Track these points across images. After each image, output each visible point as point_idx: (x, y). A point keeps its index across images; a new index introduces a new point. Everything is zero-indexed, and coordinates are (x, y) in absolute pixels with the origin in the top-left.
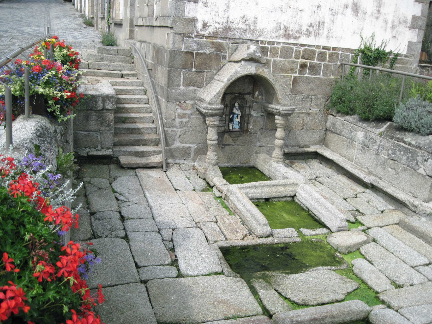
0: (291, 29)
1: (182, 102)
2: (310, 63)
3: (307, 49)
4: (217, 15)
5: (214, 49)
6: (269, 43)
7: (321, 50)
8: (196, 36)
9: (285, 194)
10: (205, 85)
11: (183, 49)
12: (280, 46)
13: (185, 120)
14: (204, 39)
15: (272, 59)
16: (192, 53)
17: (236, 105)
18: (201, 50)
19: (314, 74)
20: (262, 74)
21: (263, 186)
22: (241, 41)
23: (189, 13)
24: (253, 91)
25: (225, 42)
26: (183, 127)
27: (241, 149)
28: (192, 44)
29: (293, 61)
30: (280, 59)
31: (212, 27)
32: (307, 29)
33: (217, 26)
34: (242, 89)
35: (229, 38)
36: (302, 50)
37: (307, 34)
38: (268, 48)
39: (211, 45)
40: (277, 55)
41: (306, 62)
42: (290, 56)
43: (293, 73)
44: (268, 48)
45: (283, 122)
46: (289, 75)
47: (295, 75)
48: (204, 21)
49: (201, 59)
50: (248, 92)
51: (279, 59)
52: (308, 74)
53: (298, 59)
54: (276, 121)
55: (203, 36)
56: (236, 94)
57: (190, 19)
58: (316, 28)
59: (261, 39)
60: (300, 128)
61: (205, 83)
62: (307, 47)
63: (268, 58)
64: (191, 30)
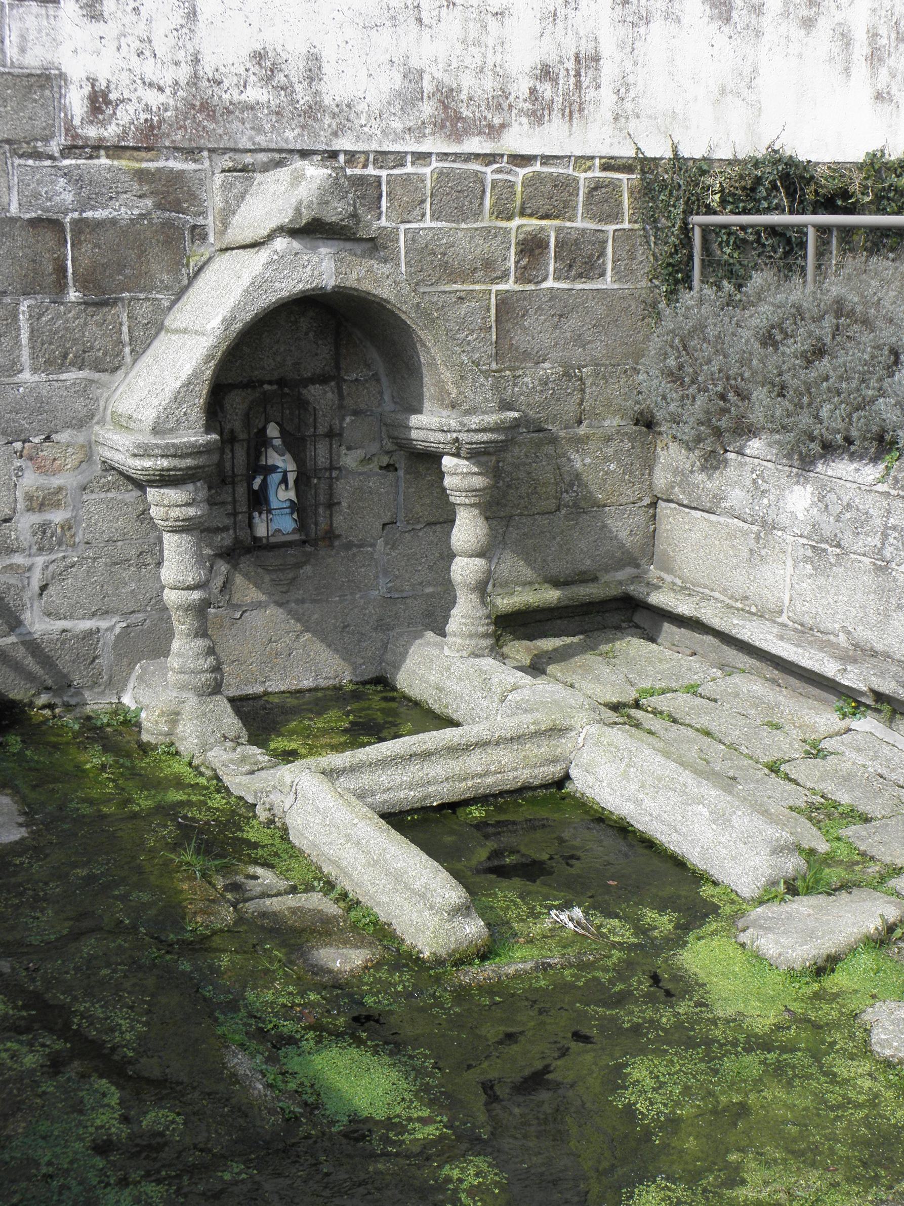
0: (464, 96)
1: (36, 440)
2: (558, 230)
3: (539, 173)
4: (147, 53)
5: (149, 202)
6: (381, 157)
7: (598, 174)
8: (68, 151)
9: (524, 775)
10: (128, 359)
11: (14, 210)
12: (427, 171)
13: (57, 517)
14: (104, 161)
15: (403, 227)
16: (55, 225)
17: (273, 431)
18: (93, 208)
19: (580, 276)
20: (367, 286)
21: (426, 756)
22: (263, 157)
23: (23, 50)
24: (338, 367)
25: (190, 166)
26: (51, 550)
27: (316, 616)
29: (488, 229)
32: (533, 91)
33: (154, 99)
35: (212, 151)
36: (519, 180)
37: (534, 113)
39: (136, 186)
40: (417, 212)
41: (542, 229)
42: (475, 206)
43: (493, 281)
45: (479, 482)
46: (477, 287)
47: (502, 287)
48: (93, 81)
49: (97, 246)
50: (318, 371)
52: (557, 278)
53: (509, 218)
54: (448, 481)
55: (96, 148)
56: (267, 387)
57: (30, 75)
58: (566, 83)
59: (345, 143)
60: (551, 504)
61: (127, 350)
62: (538, 167)
63: (383, 222)
64: (39, 123)
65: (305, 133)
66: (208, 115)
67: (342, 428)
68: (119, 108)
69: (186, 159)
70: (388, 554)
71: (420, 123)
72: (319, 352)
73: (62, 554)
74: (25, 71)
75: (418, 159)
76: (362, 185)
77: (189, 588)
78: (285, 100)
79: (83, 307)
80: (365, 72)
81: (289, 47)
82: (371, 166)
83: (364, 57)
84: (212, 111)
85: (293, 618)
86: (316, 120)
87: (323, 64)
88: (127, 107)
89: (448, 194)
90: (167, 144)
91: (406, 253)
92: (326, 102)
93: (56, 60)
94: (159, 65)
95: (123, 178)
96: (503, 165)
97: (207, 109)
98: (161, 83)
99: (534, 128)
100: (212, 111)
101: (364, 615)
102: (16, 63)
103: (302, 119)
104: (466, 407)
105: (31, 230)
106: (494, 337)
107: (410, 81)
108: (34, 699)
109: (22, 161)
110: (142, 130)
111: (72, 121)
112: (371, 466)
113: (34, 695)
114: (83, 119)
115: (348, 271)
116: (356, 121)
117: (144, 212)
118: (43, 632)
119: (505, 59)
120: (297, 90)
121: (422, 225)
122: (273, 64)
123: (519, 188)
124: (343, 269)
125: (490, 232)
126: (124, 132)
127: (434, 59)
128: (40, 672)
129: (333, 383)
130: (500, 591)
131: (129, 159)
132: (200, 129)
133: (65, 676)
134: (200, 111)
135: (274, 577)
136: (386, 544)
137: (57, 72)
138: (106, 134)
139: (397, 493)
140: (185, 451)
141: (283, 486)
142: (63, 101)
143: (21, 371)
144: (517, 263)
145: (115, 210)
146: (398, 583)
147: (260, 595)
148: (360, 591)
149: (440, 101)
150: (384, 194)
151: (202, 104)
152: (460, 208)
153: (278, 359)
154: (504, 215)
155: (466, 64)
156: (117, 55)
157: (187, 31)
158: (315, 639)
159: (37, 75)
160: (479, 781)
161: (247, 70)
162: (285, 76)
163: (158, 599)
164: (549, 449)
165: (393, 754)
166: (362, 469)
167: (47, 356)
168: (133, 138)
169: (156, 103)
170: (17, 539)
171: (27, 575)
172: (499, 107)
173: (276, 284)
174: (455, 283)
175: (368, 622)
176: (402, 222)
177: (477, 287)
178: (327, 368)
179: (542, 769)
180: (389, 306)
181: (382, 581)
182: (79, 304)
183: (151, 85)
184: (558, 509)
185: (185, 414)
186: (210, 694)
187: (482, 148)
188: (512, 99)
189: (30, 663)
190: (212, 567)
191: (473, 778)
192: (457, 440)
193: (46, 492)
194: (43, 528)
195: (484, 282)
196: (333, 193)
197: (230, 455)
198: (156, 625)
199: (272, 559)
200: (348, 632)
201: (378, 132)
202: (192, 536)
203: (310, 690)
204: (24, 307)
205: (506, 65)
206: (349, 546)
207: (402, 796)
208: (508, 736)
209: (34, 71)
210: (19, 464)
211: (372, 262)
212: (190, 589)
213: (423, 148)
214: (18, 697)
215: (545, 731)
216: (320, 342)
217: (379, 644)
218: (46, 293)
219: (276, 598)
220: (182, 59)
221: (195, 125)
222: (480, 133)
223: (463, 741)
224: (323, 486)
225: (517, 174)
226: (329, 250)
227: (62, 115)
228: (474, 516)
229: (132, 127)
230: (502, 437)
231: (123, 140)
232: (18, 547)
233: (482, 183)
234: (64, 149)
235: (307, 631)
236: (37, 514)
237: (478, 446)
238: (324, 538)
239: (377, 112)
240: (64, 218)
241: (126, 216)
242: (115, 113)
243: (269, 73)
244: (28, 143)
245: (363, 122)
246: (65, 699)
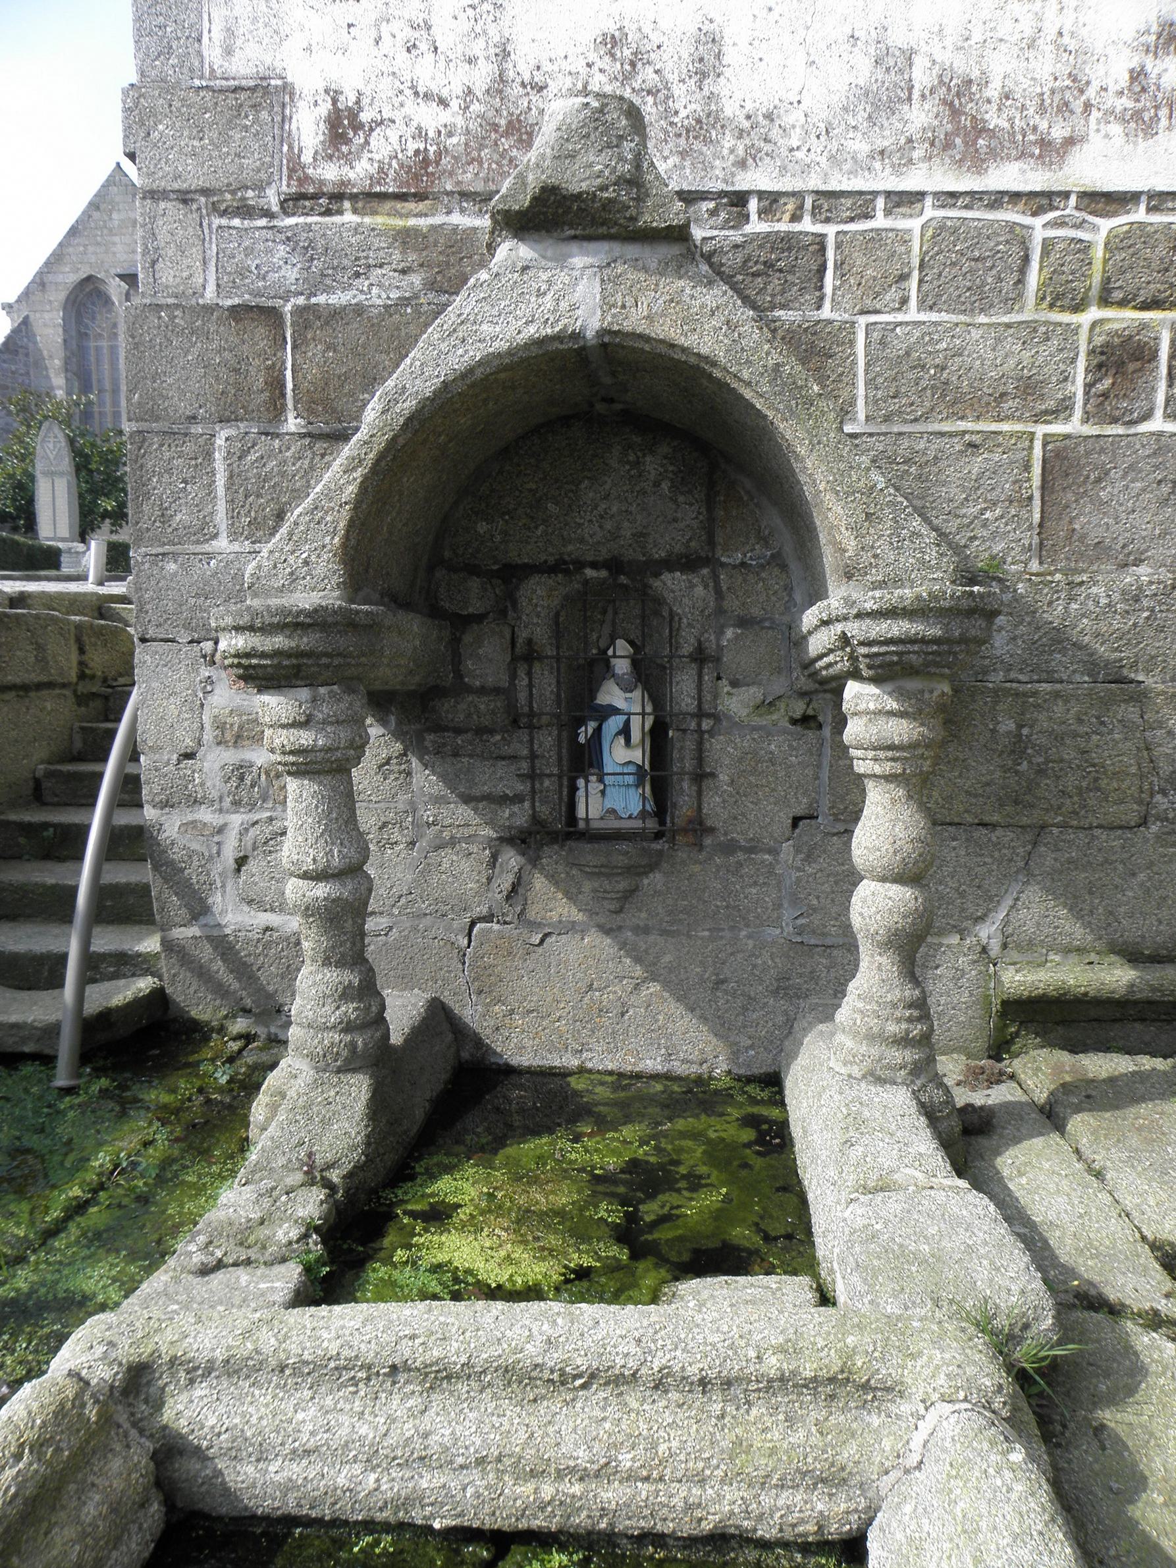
0: (993, 92)
4: (423, 46)
5: (416, 279)
8: (293, 202)
11: (210, 294)
12: (914, 225)
14: (349, 218)
15: (863, 320)
16: (271, 315)
18: (328, 290)
20: (667, 330)
23: (228, 52)
24: (711, 543)
26: (252, 807)
27: (667, 958)
28: (269, 252)
29: (1032, 326)
30: (923, 317)
31: (393, 134)
32: (1137, 75)
33: (431, 118)
34: (627, 531)
36: (1100, 239)
37: (1137, 115)
38: (820, 242)
39: (397, 255)
40: (893, 294)
41: (1144, 326)
42: (1008, 284)
43: (1038, 418)
44: (820, 240)
45: (900, 730)
46: (1005, 427)
48: (334, 95)
50: (678, 548)
51: (913, 313)
53: (1078, 308)
54: (854, 730)
55: (337, 198)
56: (589, 573)
57: (235, 90)
62: (1140, 214)
63: (826, 312)
65: (687, 163)
66: (520, 140)
67: (720, 648)
68: (375, 134)
69: (480, 211)
70: (799, 869)
71: (903, 141)
72: (679, 515)
73: (268, 814)
74: (232, 83)
75: (898, 205)
76: (790, 249)
77: (306, 876)
78: (654, 110)
79: (307, 441)
80: (801, 58)
81: (664, 25)
82: (807, 218)
83: (802, 32)
84: (527, 133)
85: (628, 955)
86: (707, 141)
87: (724, 49)
88: (388, 132)
89: (953, 264)
90: (449, 187)
91: (868, 364)
92: (728, 112)
93: (278, 65)
94: (442, 64)
95: (377, 243)
96: (1067, 212)
97: (519, 130)
98: (445, 93)
99: (1135, 144)
100: (527, 133)
101: (755, 966)
102: (219, 73)
103: (682, 141)
104: (875, 576)
105: (233, 324)
106: (1037, 517)
107: (888, 70)
108: (227, 1023)
109: (224, 221)
110: (411, 167)
111: (299, 157)
112: (775, 717)
113: (226, 1017)
114: (316, 153)
115: (629, 301)
116: (781, 142)
117: (407, 295)
118: (237, 927)
119: (1081, 20)
120: (676, 93)
121: (900, 317)
122: (635, 54)
123: (1099, 253)
124: (619, 297)
125: (1035, 330)
126: (381, 170)
127: (936, 29)
128: (235, 985)
129: (705, 571)
130: (1015, 955)
131: (388, 215)
132: (505, 162)
133: (270, 996)
134: (507, 134)
135: (596, 885)
136: (798, 851)
137: (279, 82)
138: (352, 175)
139: (819, 766)
140: (268, 620)
141: (622, 740)
142: (287, 127)
143: (215, 536)
144: (1088, 386)
145: (362, 291)
146: (816, 919)
147: (574, 911)
148: (747, 926)
149: (944, 102)
150: (830, 265)
151: (510, 122)
152: (978, 289)
153: (608, 525)
154: (1066, 302)
155: (1000, 35)
156: (374, 51)
157: (491, 8)
158: (666, 995)
159: (249, 89)
160: (577, 1489)
161: (589, 65)
162: (656, 72)
163: (410, 898)
164: (1131, 712)
165: (346, 1353)
166: (757, 721)
167: (253, 514)
168: (395, 180)
169: (434, 124)
170: (202, 784)
171: (216, 839)
172: (1064, 108)
173: (485, 327)
174: (962, 418)
175: (761, 981)
176: (863, 312)
177: (1005, 427)
178: (693, 544)
179: (784, 1498)
180: (717, 373)
181: (788, 914)
182: (302, 436)
183: (427, 96)
184: (1144, 822)
185: (306, 563)
186: (339, 1071)
187: (1026, 182)
188: (1091, 92)
189: (219, 967)
190: (494, 857)
191: (560, 1475)
192: (845, 639)
193: (245, 718)
194: (240, 771)
195: (1020, 419)
196: (587, 136)
197: (525, 682)
198: (406, 938)
199: (589, 854)
200: (726, 992)
201: (823, 160)
202: (320, 783)
203: (655, 1077)
204: (220, 441)
205: (1084, 32)
206: (730, 848)
207: (341, 1481)
208: (693, 1371)
209: (244, 83)
210: (207, 674)
211: (682, 283)
212: (312, 879)
213: (911, 182)
214: (204, 1017)
215: (815, 1379)
216: (681, 499)
217: (780, 1019)
218: (252, 419)
219: (601, 919)
220: (479, 53)
221: (496, 157)
222: (1022, 156)
223: (553, 1359)
224: (690, 744)
225: (1095, 228)
226: (588, 260)
227: (285, 148)
228: (893, 801)
229: (394, 163)
230: (934, 631)
231: (379, 183)
232: (204, 797)
233: (1024, 245)
234: (286, 200)
235: (654, 980)
236: (232, 751)
237: (883, 649)
238: (685, 831)
239: (822, 126)
240: (284, 306)
241: (379, 302)
242: (367, 143)
243: (627, 67)
244: (233, 193)
245: (795, 143)
246: (273, 1030)
